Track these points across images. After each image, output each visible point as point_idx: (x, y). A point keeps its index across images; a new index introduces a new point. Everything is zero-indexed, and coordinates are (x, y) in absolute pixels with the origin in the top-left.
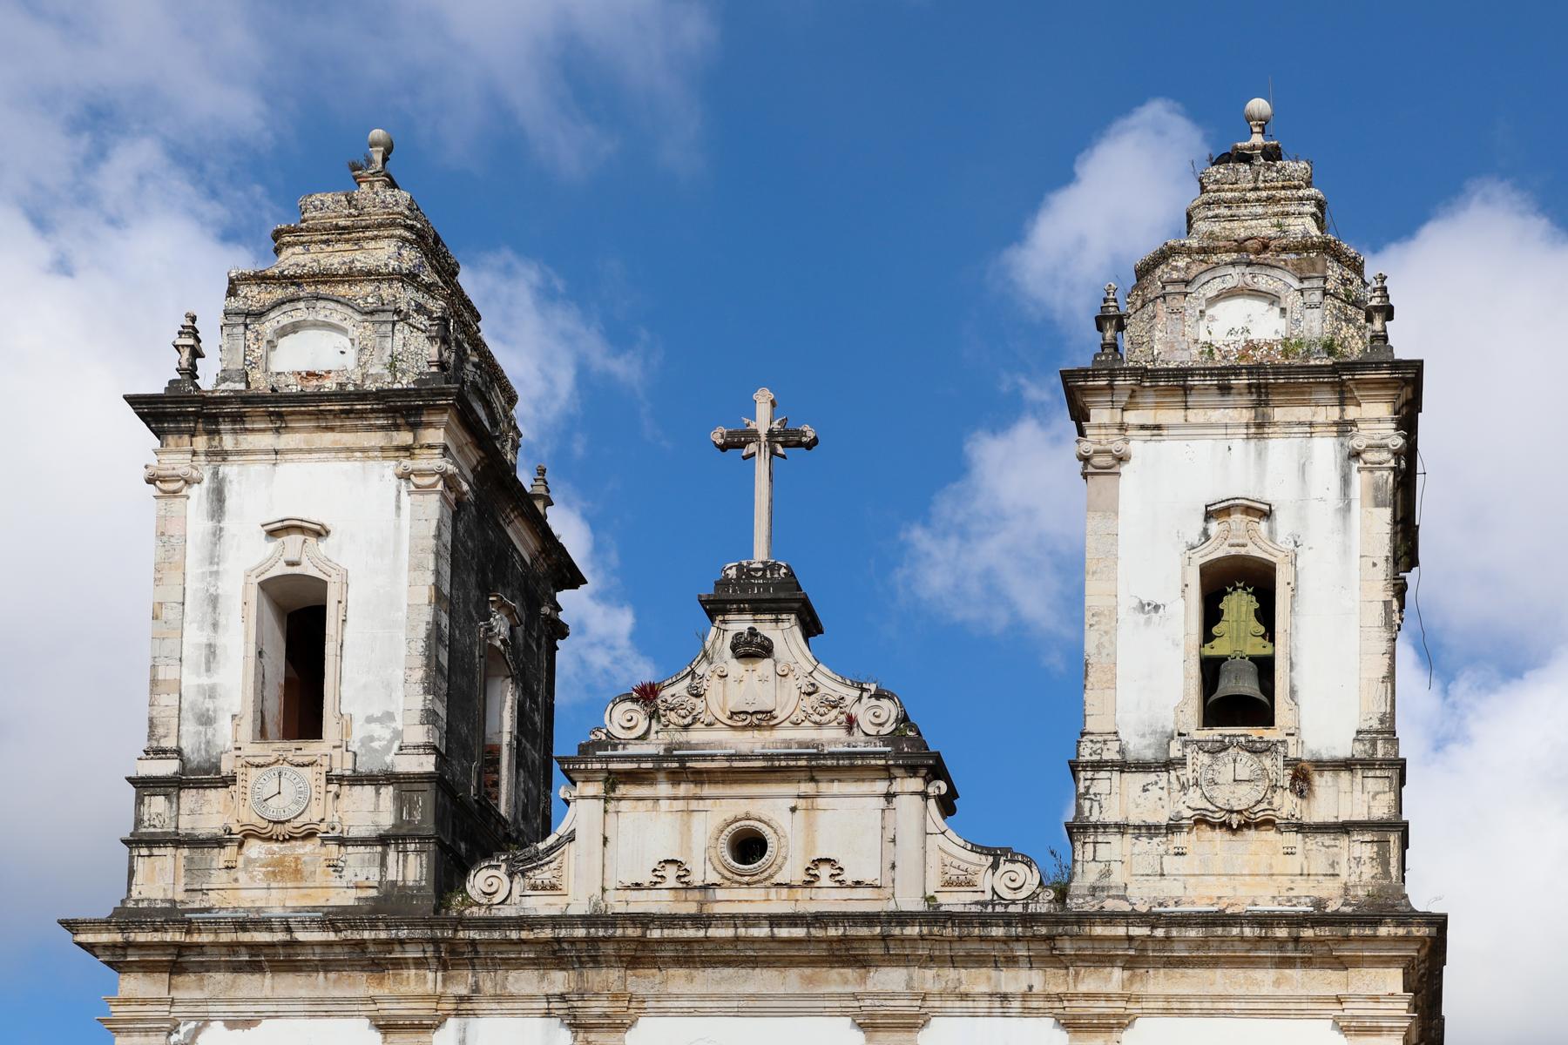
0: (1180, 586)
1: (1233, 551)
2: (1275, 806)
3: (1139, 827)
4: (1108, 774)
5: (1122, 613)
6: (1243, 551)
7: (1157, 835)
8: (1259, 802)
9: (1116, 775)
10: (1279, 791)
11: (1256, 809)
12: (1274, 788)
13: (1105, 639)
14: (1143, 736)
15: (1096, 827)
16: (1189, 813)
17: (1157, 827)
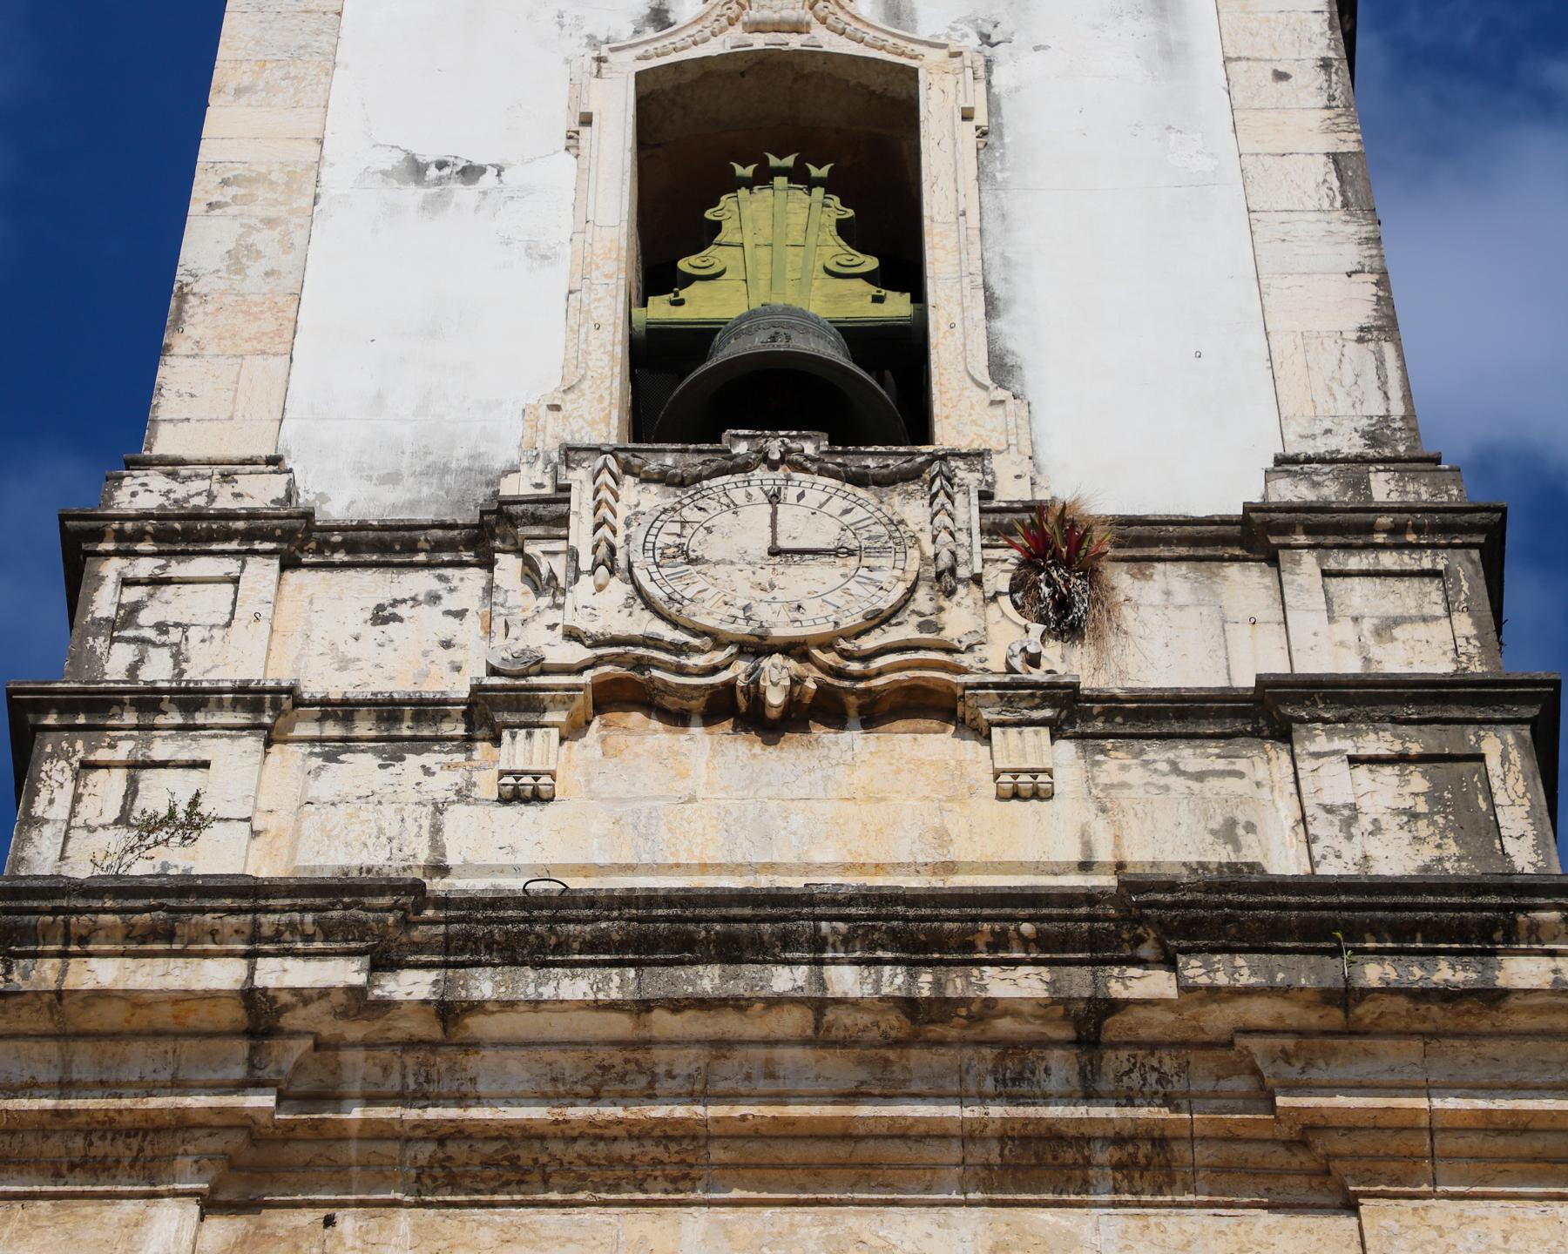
0: (568, 122)
1: (759, 42)
2: (950, 634)
3: (342, 710)
4: (230, 566)
5: (335, 181)
6: (795, 42)
7: (420, 744)
8: (880, 619)
9: (261, 573)
10: (966, 596)
11: (868, 643)
12: (945, 580)
13: (264, 239)
14: (393, 478)
15: (148, 700)
16: (577, 653)
17: (428, 709)
